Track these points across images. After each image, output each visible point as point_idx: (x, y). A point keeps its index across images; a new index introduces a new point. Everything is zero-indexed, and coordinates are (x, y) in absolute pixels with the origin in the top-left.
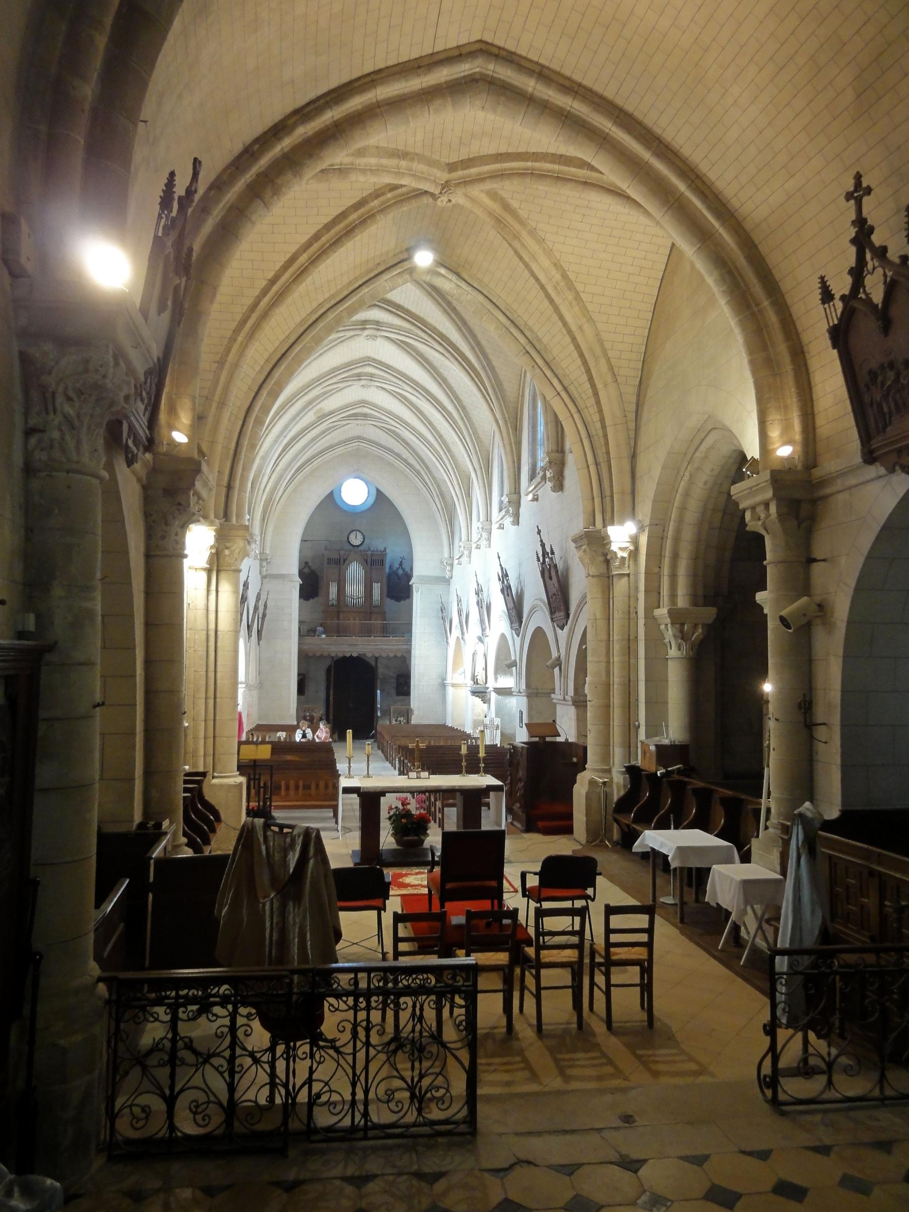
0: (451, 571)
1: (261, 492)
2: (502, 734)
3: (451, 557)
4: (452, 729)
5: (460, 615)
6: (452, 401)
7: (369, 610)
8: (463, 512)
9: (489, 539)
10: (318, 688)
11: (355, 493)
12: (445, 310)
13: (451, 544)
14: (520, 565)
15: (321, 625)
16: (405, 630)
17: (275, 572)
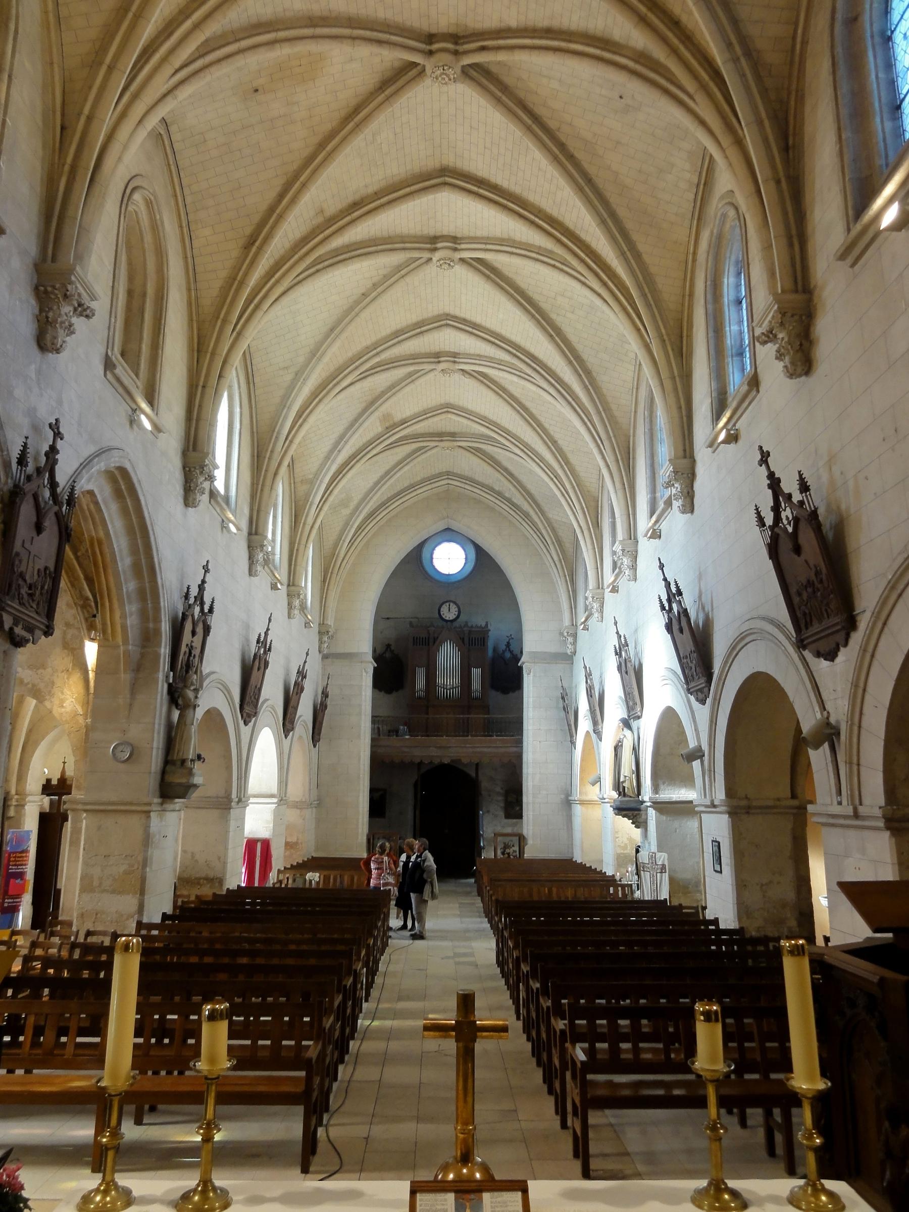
0: (575, 643)
1: (308, 528)
2: (672, 880)
3: (574, 625)
4: (582, 867)
5: (590, 695)
6: (570, 362)
7: (466, 702)
8: (591, 551)
9: (634, 568)
10: (405, 808)
11: (449, 559)
12: (556, 159)
13: (573, 608)
14: (700, 577)
15: (405, 724)
16: (513, 727)
17: (340, 650)
